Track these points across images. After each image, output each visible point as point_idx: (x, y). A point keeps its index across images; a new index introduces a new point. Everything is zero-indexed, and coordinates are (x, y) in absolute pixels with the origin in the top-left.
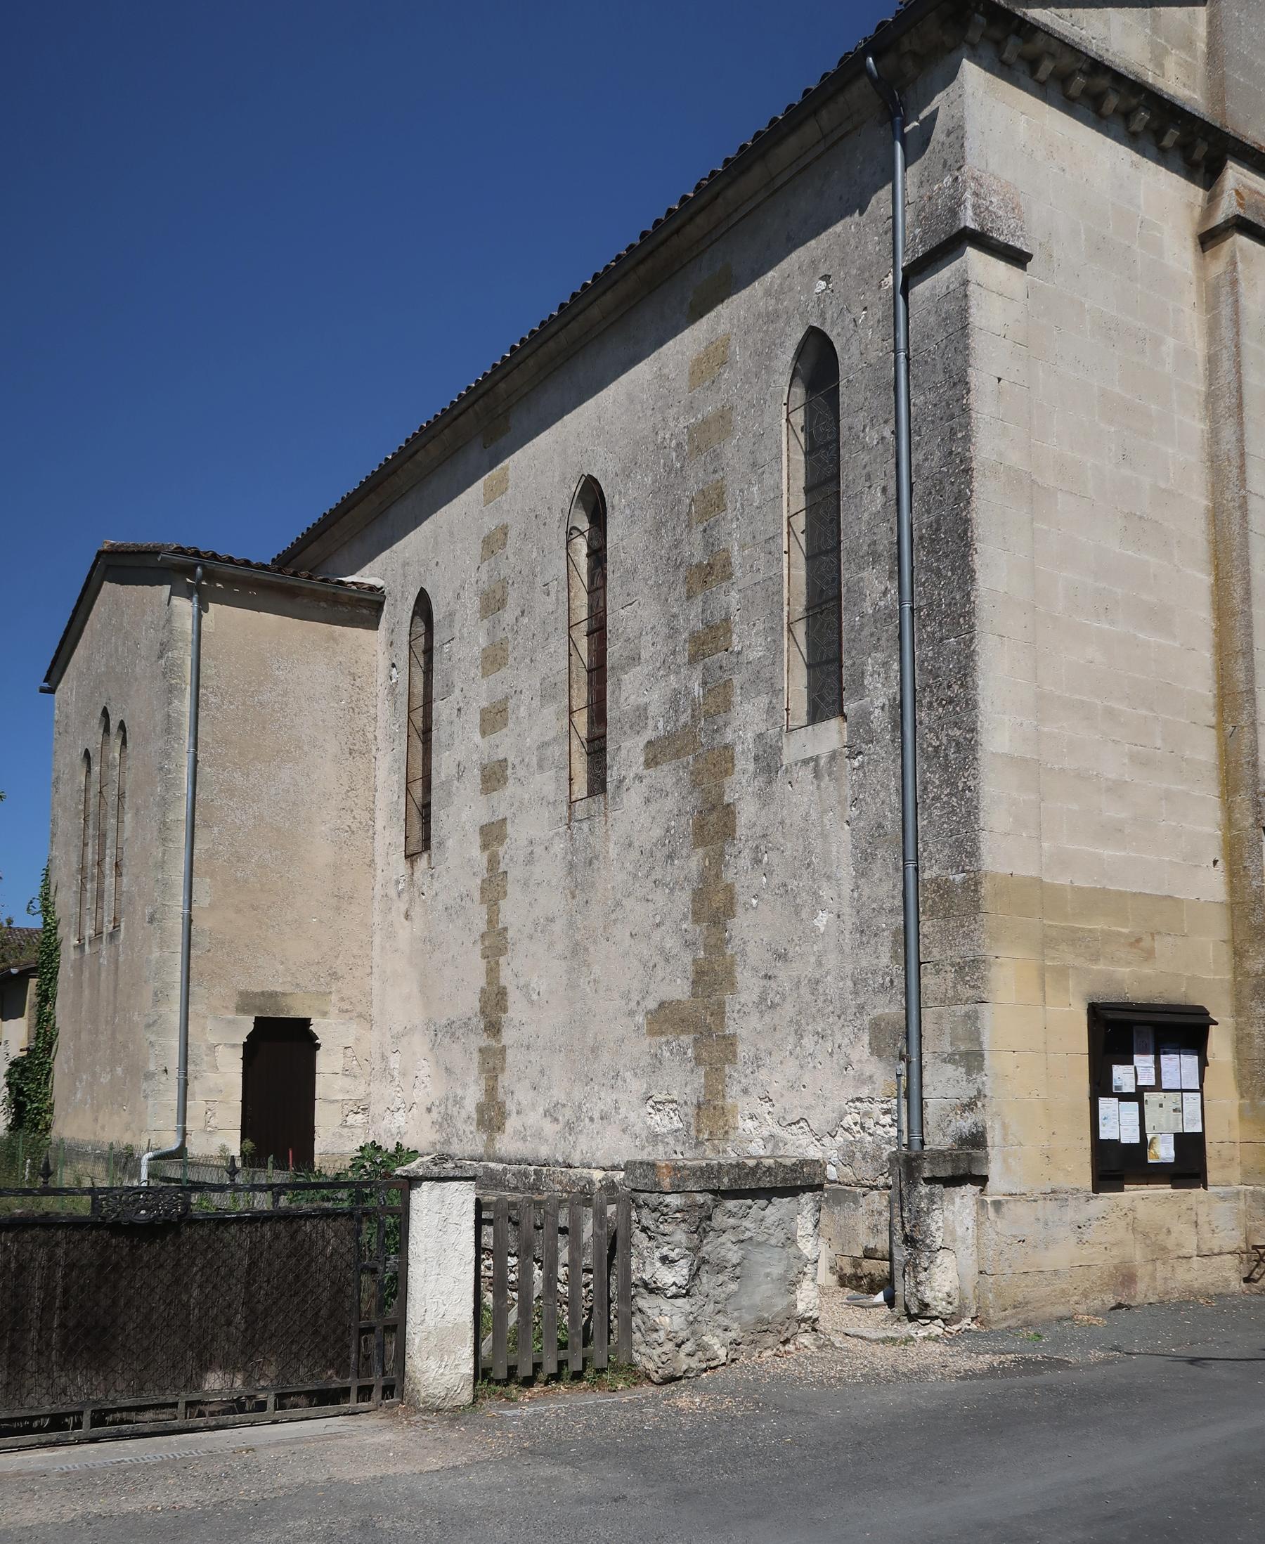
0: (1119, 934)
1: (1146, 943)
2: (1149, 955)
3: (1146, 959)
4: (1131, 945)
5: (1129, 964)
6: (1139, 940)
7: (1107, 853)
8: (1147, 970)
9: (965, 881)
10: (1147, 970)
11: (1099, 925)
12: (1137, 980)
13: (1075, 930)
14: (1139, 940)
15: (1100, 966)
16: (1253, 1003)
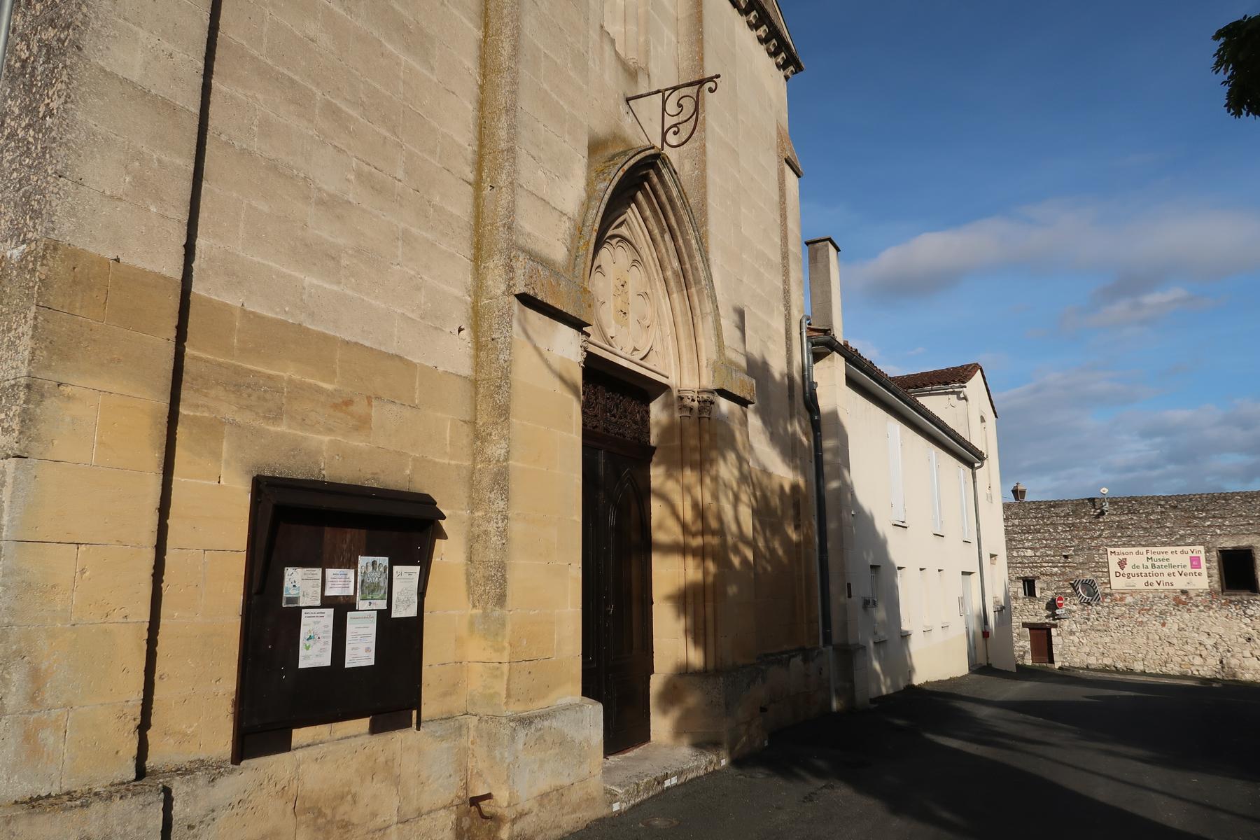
0: (320, 390)
1: (359, 407)
2: (363, 424)
3: (356, 429)
4: (335, 406)
5: (330, 430)
6: (348, 403)
7: (310, 280)
8: (358, 442)
9: (24, 257)
10: (358, 442)
11: (288, 372)
12: (334, 451)
13: (238, 371)
14: (348, 403)
15: (282, 428)
16: (492, 495)
